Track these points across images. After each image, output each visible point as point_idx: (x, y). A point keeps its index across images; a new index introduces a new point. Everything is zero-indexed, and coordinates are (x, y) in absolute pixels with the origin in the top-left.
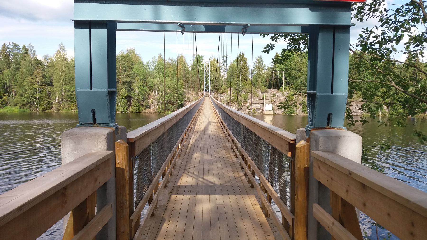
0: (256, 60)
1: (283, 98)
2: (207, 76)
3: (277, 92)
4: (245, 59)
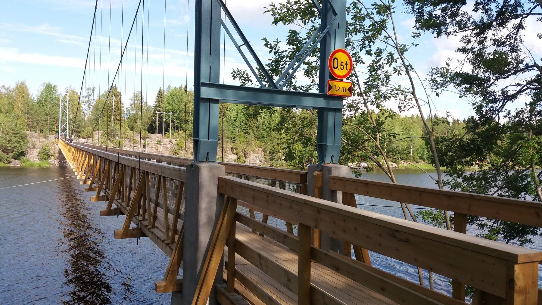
1: (171, 146)
2: (64, 113)
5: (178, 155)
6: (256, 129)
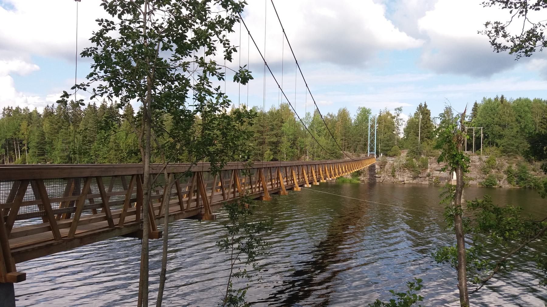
4: (427, 112)
5: (488, 173)
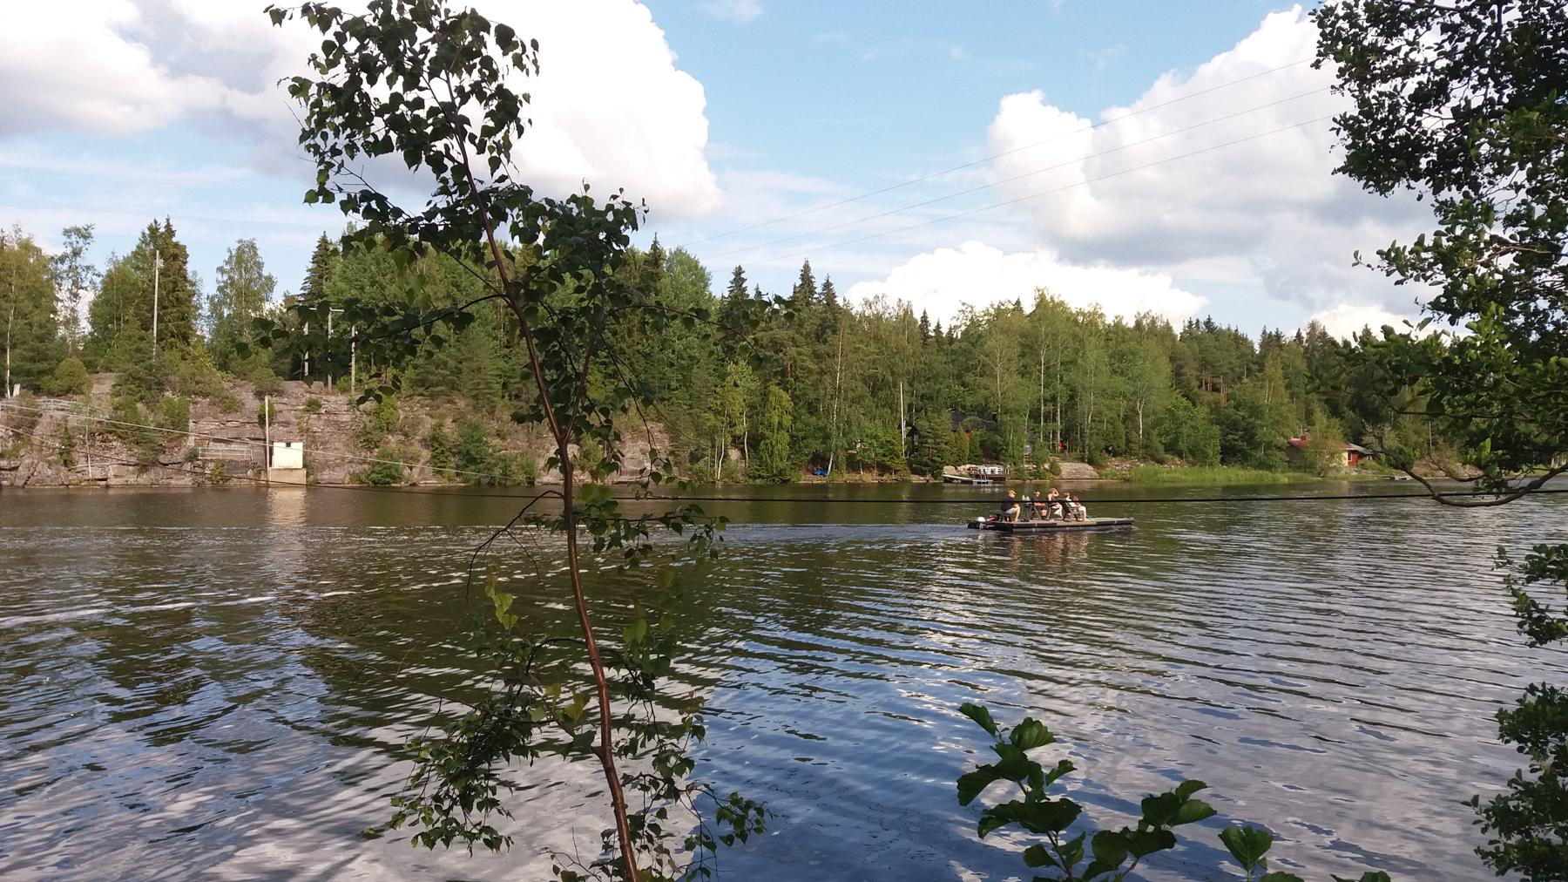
0: (231, 257)
1: (353, 420)
3: (327, 393)
4: (176, 251)
5: (377, 447)
6: (642, 361)
